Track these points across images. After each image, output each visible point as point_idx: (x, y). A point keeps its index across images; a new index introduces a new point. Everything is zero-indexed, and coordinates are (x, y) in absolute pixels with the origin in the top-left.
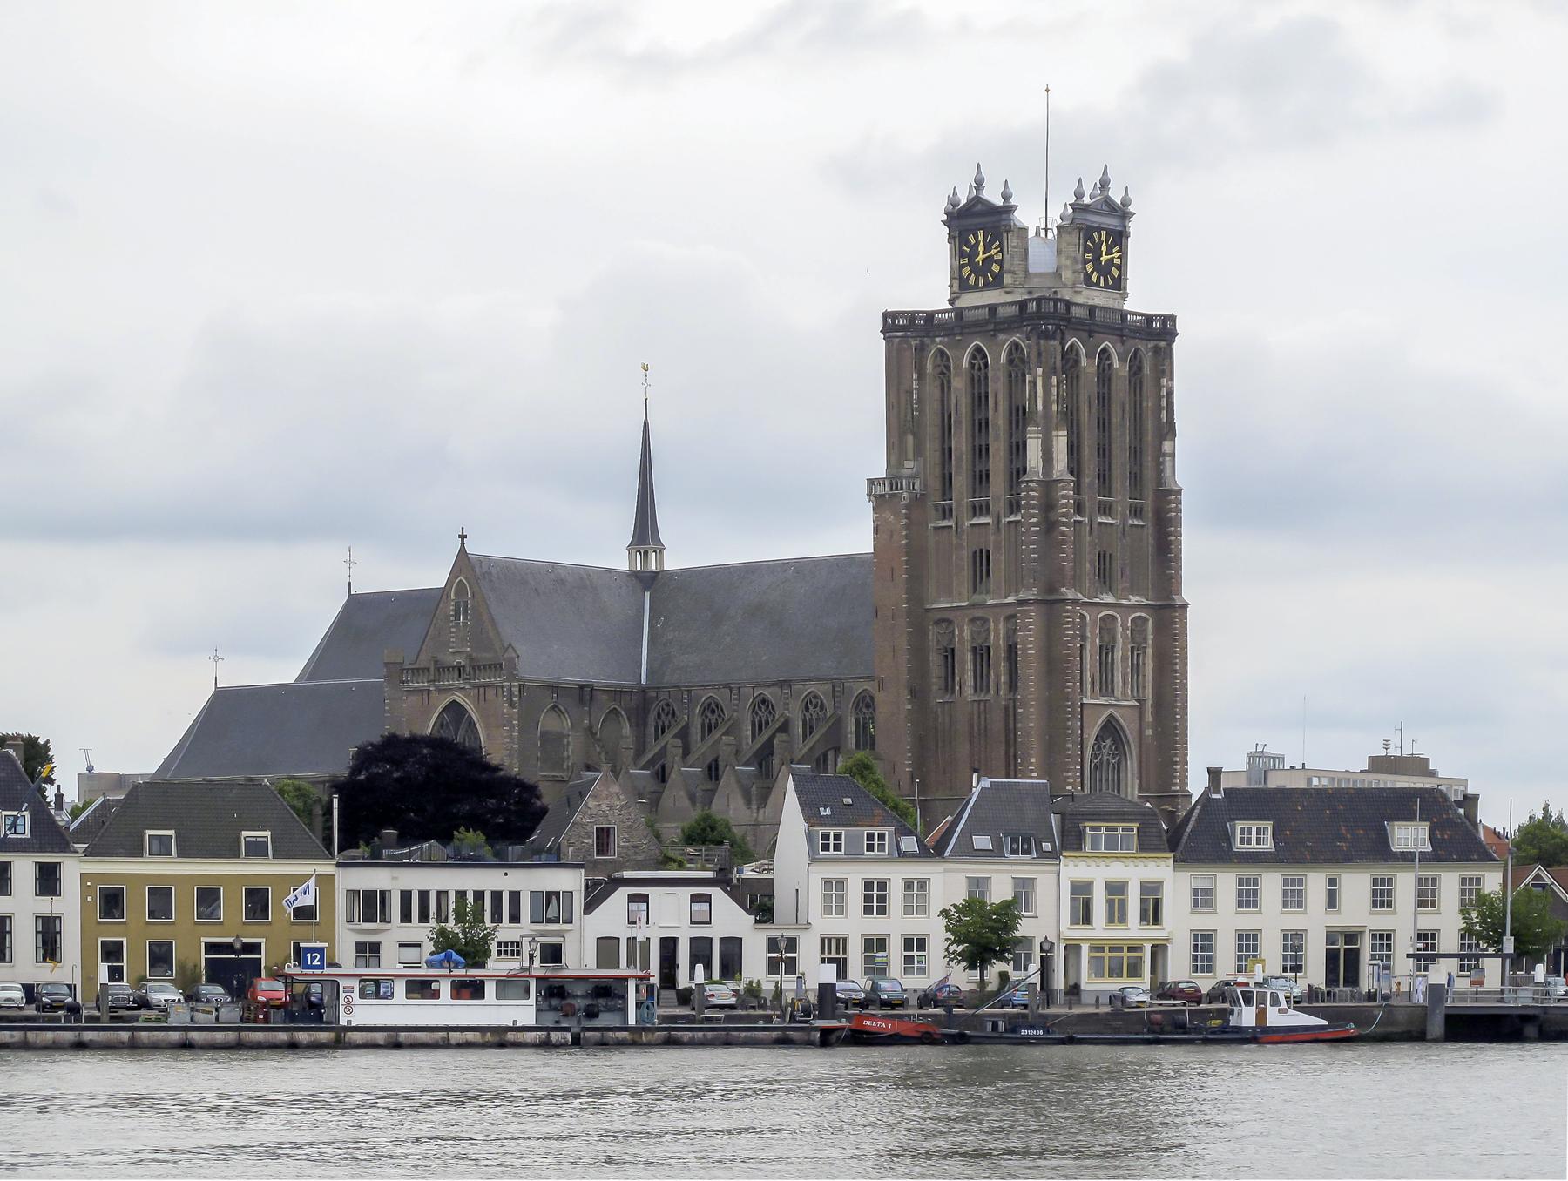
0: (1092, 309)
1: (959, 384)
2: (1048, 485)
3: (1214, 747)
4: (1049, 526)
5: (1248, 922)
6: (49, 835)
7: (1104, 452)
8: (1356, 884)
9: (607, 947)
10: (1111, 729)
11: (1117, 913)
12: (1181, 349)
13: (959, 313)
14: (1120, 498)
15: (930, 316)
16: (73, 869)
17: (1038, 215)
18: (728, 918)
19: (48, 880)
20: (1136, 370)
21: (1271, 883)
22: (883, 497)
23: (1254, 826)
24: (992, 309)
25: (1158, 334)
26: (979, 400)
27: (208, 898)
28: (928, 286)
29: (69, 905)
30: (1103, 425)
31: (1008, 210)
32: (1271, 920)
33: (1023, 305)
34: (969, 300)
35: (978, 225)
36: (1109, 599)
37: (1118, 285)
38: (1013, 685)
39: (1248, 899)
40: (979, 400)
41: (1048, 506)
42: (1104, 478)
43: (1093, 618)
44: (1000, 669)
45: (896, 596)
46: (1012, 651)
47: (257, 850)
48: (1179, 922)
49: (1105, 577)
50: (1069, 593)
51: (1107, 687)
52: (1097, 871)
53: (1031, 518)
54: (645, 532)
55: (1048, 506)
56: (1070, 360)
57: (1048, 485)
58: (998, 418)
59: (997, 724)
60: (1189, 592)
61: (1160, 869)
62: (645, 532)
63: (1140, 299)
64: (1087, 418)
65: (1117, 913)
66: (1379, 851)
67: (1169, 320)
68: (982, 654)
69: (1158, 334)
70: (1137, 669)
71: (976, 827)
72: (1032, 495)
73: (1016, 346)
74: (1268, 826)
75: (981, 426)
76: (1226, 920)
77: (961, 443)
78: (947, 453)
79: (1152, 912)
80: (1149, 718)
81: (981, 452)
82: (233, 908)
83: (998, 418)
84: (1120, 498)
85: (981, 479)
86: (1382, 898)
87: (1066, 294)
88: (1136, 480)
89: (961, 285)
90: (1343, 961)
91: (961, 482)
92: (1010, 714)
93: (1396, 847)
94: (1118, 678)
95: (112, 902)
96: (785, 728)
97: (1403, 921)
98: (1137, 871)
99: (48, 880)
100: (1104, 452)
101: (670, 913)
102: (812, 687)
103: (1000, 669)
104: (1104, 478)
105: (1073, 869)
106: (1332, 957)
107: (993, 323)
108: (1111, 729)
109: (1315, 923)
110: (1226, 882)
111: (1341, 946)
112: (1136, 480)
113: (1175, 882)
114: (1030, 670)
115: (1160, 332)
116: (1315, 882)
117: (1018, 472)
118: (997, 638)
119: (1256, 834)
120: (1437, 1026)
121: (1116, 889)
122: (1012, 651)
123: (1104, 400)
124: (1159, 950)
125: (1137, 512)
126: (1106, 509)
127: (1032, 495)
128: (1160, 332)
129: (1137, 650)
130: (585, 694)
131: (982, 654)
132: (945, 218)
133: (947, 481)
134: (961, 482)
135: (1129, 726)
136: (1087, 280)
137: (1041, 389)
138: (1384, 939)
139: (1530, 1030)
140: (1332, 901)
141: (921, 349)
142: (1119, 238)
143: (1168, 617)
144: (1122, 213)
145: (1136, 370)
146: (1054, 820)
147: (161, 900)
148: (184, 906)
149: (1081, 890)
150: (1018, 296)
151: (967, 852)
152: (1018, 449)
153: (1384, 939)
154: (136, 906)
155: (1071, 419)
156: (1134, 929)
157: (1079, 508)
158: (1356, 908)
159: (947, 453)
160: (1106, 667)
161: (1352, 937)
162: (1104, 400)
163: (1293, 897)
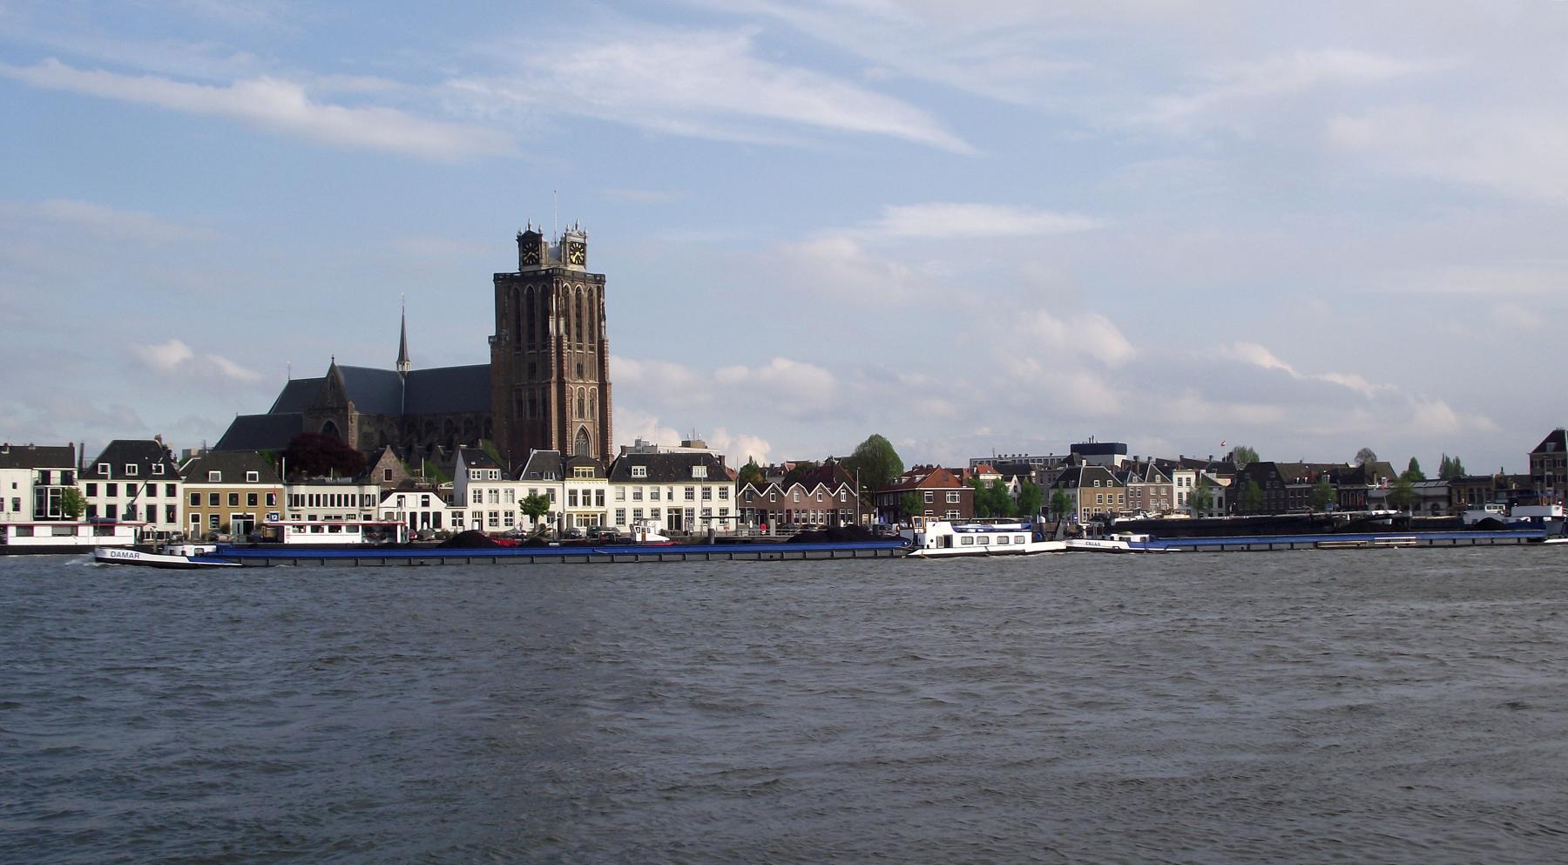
1: (523, 300)
3: (621, 439)
6: (172, 474)
7: (579, 326)
8: (679, 490)
9: (389, 515)
10: (583, 430)
11: (587, 502)
12: (608, 288)
14: (586, 343)
16: (180, 487)
18: (436, 504)
19: (171, 491)
21: (647, 489)
22: (495, 342)
27: (234, 499)
28: (512, 266)
29: (179, 501)
30: (579, 316)
32: (647, 505)
39: (638, 496)
42: (579, 336)
47: (253, 477)
48: (611, 505)
51: (581, 414)
52: (578, 485)
61: (603, 484)
62: (402, 358)
65: (587, 502)
76: (630, 505)
77: (524, 323)
78: (519, 326)
79: (601, 501)
84: (586, 343)
85: (532, 336)
86: (690, 495)
89: (523, 263)
90: (676, 518)
91: (524, 337)
95: (196, 499)
97: (697, 504)
98: (594, 485)
99: (171, 491)
100: (579, 326)
101: (413, 501)
104: (579, 336)
105: (570, 484)
106: (670, 518)
108: (583, 430)
109: (664, 505)
110: (630, 489)
113: (610, 490)
115: (599, 280)
116: (664, 489)
119: (639, 471)
123: (579, 306)
124: (603, 517)
125: (592, 349)
126: (580, 348)
128: (599, 280)
134: (524, 337)
138: (691, 512)
140: (670, 496)
147: (215, 499)
149: (573, 493)
153: (691, 512)
154: (206, 501)
156: (594, 508)
158: (680, 500)
159: (519, 326)
161: (678, 511)
162: (579, 306)
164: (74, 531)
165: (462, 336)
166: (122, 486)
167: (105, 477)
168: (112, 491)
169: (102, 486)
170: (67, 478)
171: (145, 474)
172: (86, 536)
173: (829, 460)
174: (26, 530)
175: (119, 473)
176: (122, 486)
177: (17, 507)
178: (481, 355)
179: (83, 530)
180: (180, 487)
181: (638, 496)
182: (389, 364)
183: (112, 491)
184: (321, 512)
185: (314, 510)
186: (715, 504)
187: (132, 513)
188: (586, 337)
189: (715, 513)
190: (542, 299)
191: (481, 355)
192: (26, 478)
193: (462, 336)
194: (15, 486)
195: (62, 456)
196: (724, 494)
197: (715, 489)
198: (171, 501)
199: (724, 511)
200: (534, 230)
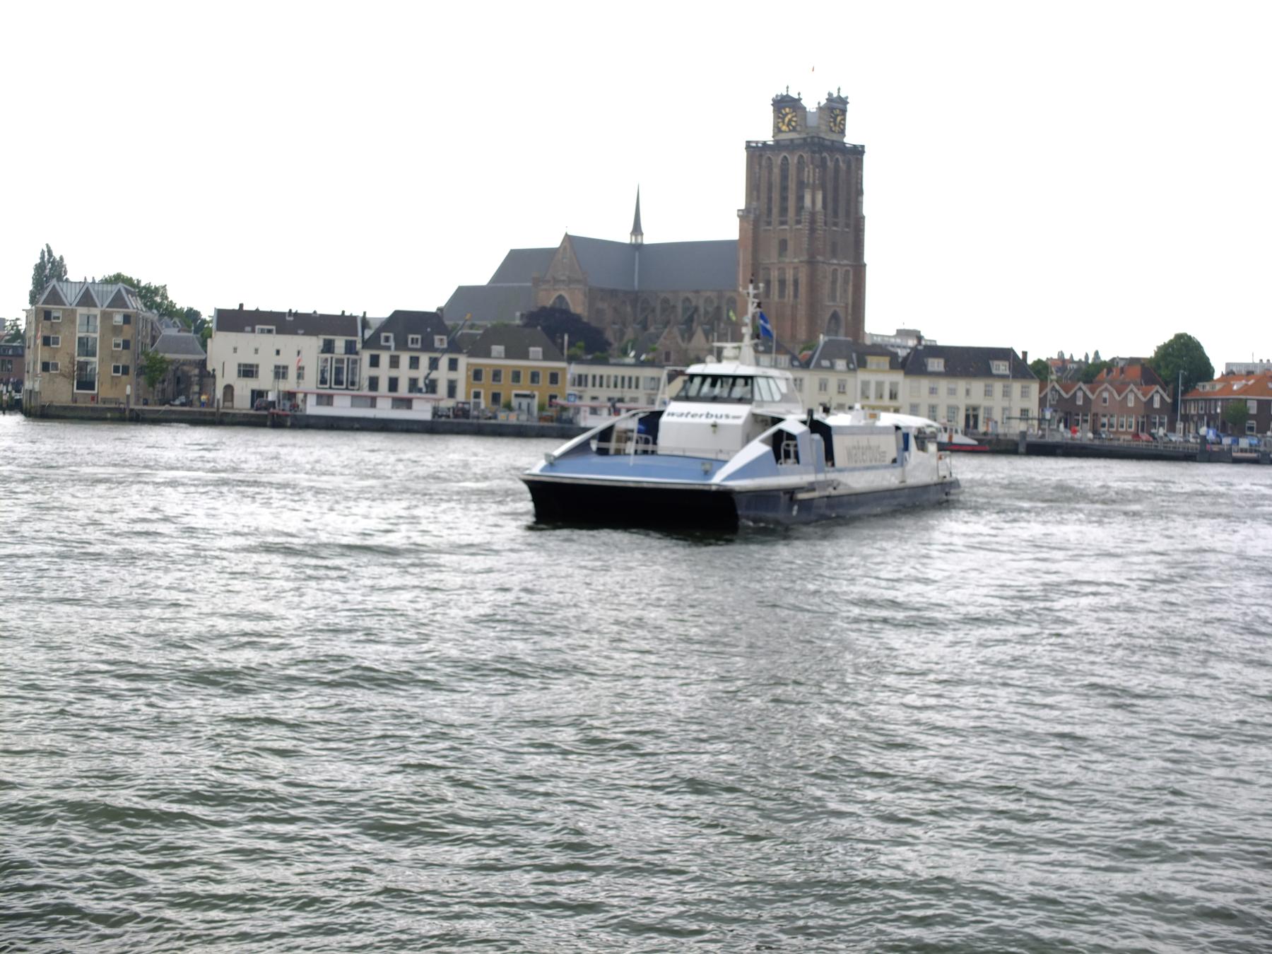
0: (833, 142)
1: (776, 171)
2: (813, 214)
4: (812, 230)
5: (394, 373)
6: (454, 347)
7: (836, 200)
8: (978, 386)
10: (835, 316)
12: (867, 159)
13: (777, 142)
14: (841, 219)
15: (764, 143)
16: (463, 361)
17: (812, 102)
19: (453, 365)
20: (849, 167)
21: (943, 385)
22: (744, 216)
23: (415, 336)
24: (792, 140)
25: (857, 152)
26: (784, 177)
27: (516, 376)
28: (764, 132)
29: (461, 375)
31: (800, 99)
33: (805, 139)
34: (781, 136)
35: (785, 106)
36: (835, 261)
37: (842, 132)
38: (796, 296)
40: (784, 177)
41: (813, 222)
43: (829, 269)
44: (790, 290)
45: (744, 257)
46: (796, 283)
49: (834, 253)
50: (820, 258)
51: (833, 298)
53: (804, 227)
54: (637, 229)
55: (813, 222)
56: (823, 160)
57: (813, 214)
58: (792, 185)
59: (788, 312)
60: (867, 259)
61: (898, 377)
62: (637, 229)
63: (850, 139)
64: (830, 186)
66: (986, 373)
67: (863, 147)
68: (782, 283)
69: (857, 152)
70: (845, 291)
71: (823, 356)
72: (805, 217)
73: (801, 156)
74: (445, 337)
75: (784, 188)
77: (776, 196)
78: (770, 199)
80: (850, 311)
81: (784, 199)
82: (526, 378)
83: (792, 185)
84: (841, 219)
85: (784, 210)
86: (988, 393)
87: (822, 135)
88: (848, 214)
89: (777, 130)
90: (972, 418)
91: (775, 210)
92: (794, 307)
93: (930, 368)
94: (838, 294)
95: (477, 375)
96: (653, 310)
99: (453, 365)
100: (836, 200)
102: (708, 294)
103: (790, 290)
105: (862, 376)
106: (967, 417)
107: (791, 146)
108: (835, 316)
110: (925, 384)
111: (971, 412)
112: (848, 214)
114: (803, 290)
115: (858, 152)
117: (800, 208)
118: (789, 276)
119: (936, 364)
120: (1022, 449)
121: (880, 385)
122: (796, 283)
123: (836, 178)
125: (847, 226)
126: (835, 224)
127: (805, 217)
128: (858, 152)
129: (846, 282)
130: (613, 293)
131: (782, 283)
132: (823, 102)
133: (770, 210)
134: (775, 210)
135: (842, 315)
136: (831, 130)
137: (810, 174)
139: (1059, 451)
140: (968, 392)
141: (761, 156)
142: (844, 112)
143: (859, 270)
144: (844, 102)
145: (849, 167)
146: (854, 355)
147: (496, 375)
148: (506, 378)
149: (865, 385)
150: (803, 135)
151: (819, 366)
152: (800, 198)
154: (487, 376)
155: (823, 187)
157: (826, 223)
159: (770, 199)
160: (833, 290)
161: (975, 409)
162: (836, 178)
163: (952, 392)
164: (373, 402)
165: (702, 205)
166: (405, 358)
167: (388, 348)
168: (394, 363)
169: (385, 358)
170: (350, 348)
171: (428, 346)
172: (384, 410)
173: (1113, 359)
174: (325, 400)
175: (402, 345)
176: (405, 358)
177: (300, 376)
178: (727, 229)
179: (379, 402)
180: (463, 361)
181: (933, 391)
182: (625, 237)
183: (394, 363)
184: (604, 394)
185: (596, 391)
186: (1017, 404)
187: (432, 387)
188: (841, 212)
189: (1017, 413)
190: (809, 176)
191: (727, 229)
192: (311, 345)
193: (702, 205)
194: (278, 352)
195: (344, 324)
196: (1025, 394)
197: (1016, 387)
198: (453, 375)
199: (1024, 412)
200: (843, 95)
